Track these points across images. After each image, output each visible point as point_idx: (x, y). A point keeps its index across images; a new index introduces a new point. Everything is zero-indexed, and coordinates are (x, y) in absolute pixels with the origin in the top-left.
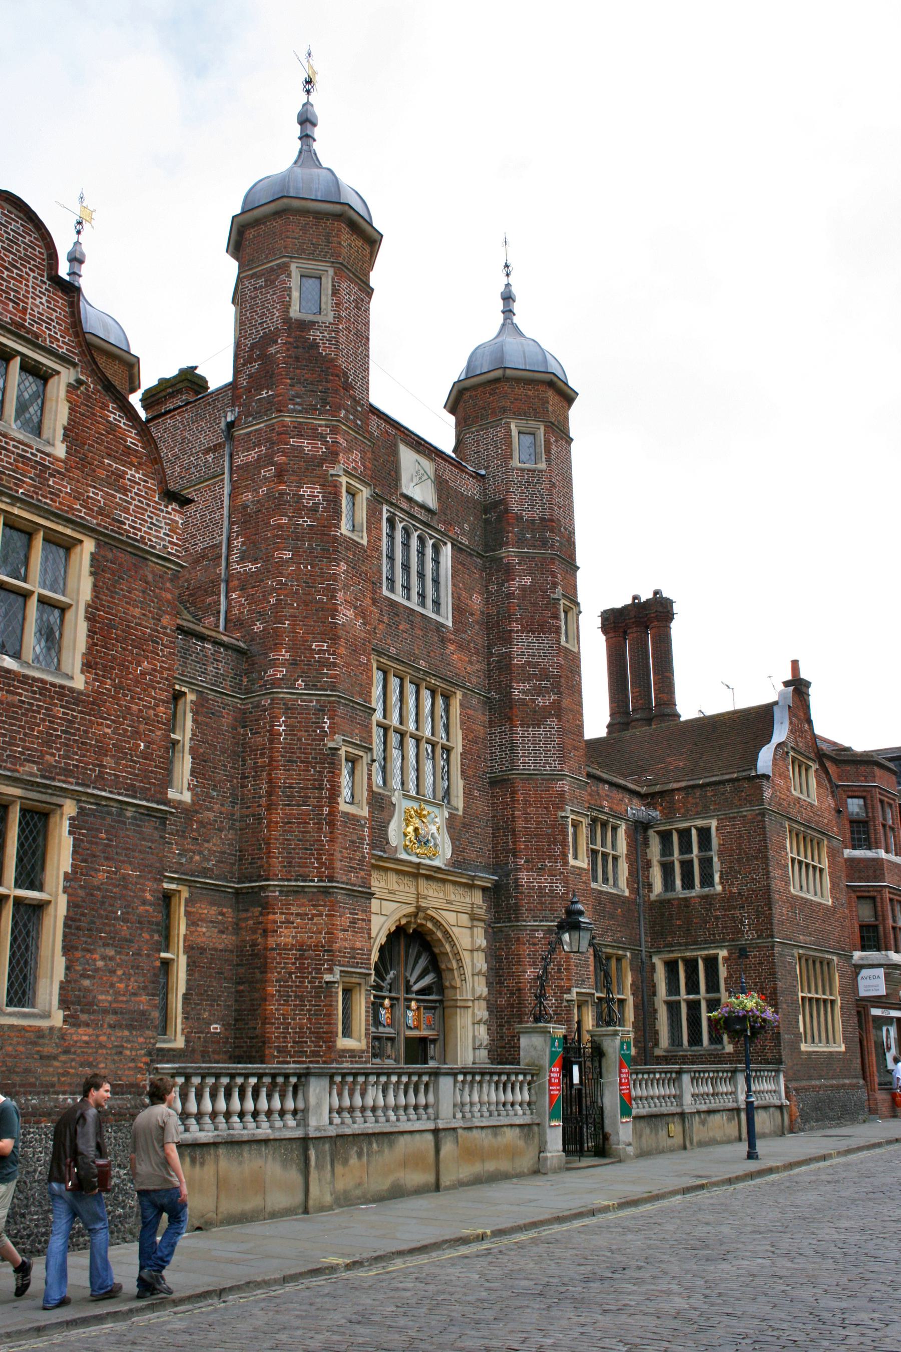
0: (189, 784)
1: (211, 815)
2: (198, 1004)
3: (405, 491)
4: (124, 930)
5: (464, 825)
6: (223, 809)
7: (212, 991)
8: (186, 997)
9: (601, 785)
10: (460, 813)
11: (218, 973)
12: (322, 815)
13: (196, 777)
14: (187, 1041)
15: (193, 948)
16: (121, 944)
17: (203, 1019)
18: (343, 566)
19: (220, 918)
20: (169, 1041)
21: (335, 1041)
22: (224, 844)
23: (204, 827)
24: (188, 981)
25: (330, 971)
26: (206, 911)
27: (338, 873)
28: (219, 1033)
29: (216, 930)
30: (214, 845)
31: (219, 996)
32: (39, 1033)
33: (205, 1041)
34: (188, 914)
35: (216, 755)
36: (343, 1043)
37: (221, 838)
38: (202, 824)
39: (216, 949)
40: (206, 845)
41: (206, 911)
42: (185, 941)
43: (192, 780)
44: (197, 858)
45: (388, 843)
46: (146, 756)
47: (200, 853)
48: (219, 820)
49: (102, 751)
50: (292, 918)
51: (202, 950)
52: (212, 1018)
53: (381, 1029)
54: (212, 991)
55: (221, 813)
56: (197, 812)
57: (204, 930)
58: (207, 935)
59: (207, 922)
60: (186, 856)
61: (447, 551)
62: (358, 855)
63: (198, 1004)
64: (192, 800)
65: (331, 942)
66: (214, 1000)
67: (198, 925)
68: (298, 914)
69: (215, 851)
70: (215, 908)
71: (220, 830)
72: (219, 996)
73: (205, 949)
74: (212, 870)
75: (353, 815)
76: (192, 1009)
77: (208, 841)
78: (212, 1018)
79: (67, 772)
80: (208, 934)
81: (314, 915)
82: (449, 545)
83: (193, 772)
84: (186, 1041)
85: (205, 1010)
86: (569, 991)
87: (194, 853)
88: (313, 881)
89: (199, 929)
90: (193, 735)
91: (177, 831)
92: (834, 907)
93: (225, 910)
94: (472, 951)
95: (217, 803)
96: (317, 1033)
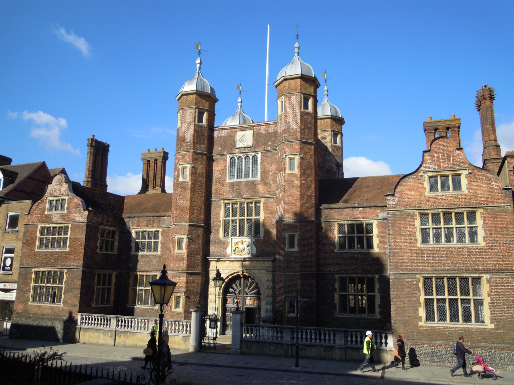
1: (166, 256)
3: (238, 146)
4: (73, 290)
9: (355, 210)
10: (262, 238)
16: (73, 292)
18: (180, 190)
32: (59, 307)
38: (163, 259)
46: (79, 259)
49: (71, 260)
61: (259, 155)
62: (182, 263)
79: (65, 265)
82: (260, 153)
92: (490, 248)
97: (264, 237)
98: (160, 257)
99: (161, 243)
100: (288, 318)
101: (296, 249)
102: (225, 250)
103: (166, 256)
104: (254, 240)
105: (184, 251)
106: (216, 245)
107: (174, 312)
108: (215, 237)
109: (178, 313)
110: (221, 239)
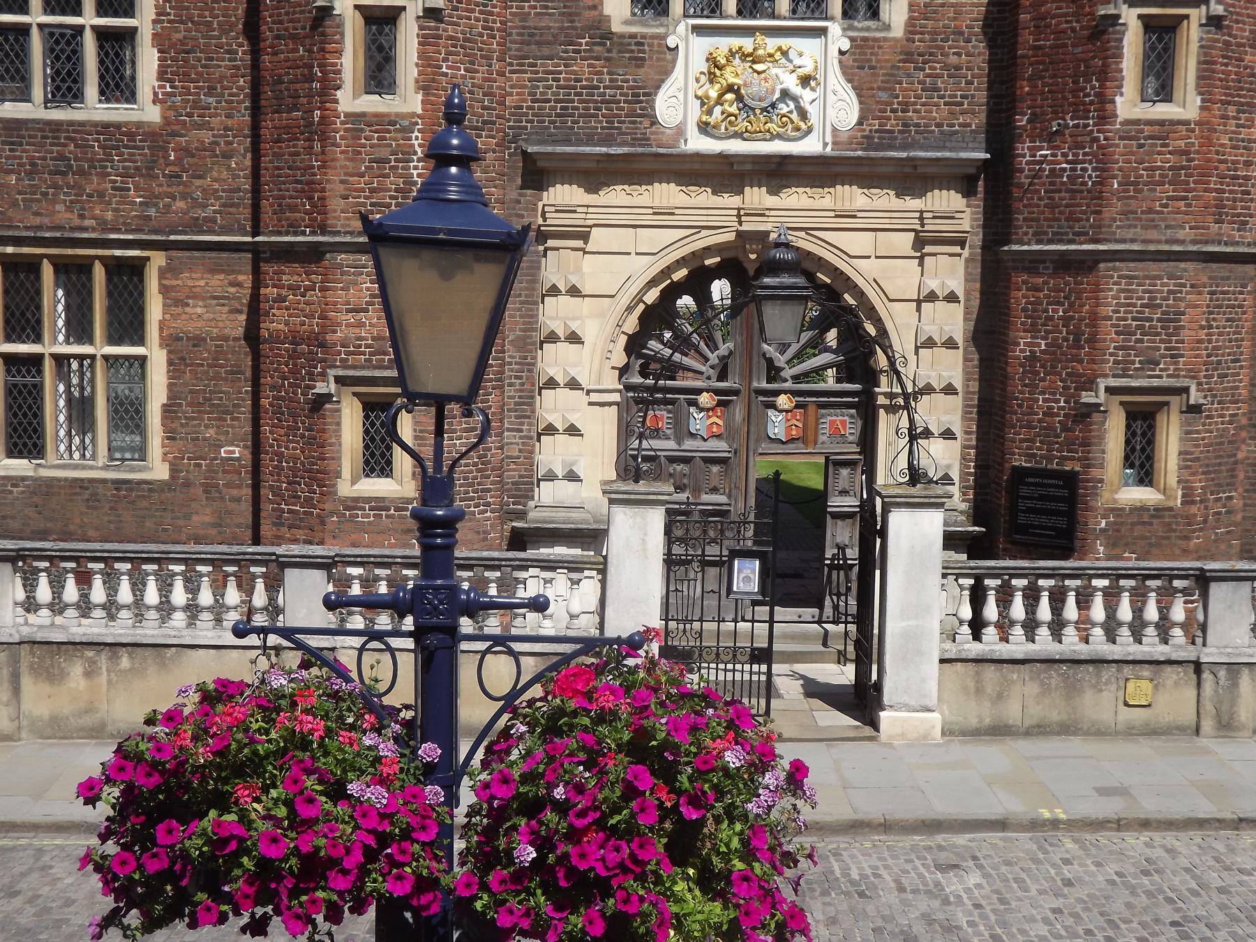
0: (155, 94)
2: (194, 419)
5: (908, 56)
6: (230, 122)
7: (221, 399)
8: (168, 411)
10: (898, 31)
11: (232, 373)
12: (312, 123)
13: (169, 81)
14: (174, 471)
15: (178, 339)
17: (205, 439)
19: (232, 290)
20: (145, 469)
21: (334, 485)
22: (235, 177)
23: (193, 156)
24: (170, 387)
25: (323, 375)
26: (202, 283)
27: (338, 218)
28: (238, 459)
29: (226, 309)
30: (215, 180)
31: (238, 406)
33: (209, 471)
34: (164, 290)
35: (211, 38)
36: (354, 485)
37: (229, 168)
38: (186, 151)
39: (226, 339)
40: (198, 182)
41: (202, 283)
42: (161, 329)
43: (160, 87)
44: (180, 204)
45: (654, 122)
47: (184, 197)
48: (222, 141)
50: (284, 292)
51: (198, 341)
52: (222, 438)
53: (689, 444)
54: (221, 399)
55: (226, 129)
56: (174, 134)
57: (199, 310)
58: (199, 318)
59: (203, 299)
60: (156, 205)
63: (194, 419)
64: (164, 117)
65: (324, 330)
66: (226, 412)
67: (187, 305)
68: (290, 288)
69: (216, 191)
70: (222, 276)
71: (227, 156)
72: (238, 406)
73: (204, 340)
74: (214, 221)
75: (376, 115)
76: (182, 425)
77: (201, 177)
78: (222, 438)
80: (206, 317)
81: (308, 289)
83: (161, 75)
84: (171, 470)
85: (207, 427)
86: (1090, 385)
87: (174, 198)
88: (303, 233)
89: (188, 309)
90: (158, 14)
91: (137, 168)
93: (241, 278)
94: (919, 302)
95: (216, 115)
96: (310, 471)
97: (911, 25)
98: (155, 138)
99: (159, 40)
100: (1118, 511)
101: (1186, 106)
102: (643, 98)
103: (207, 137)
104: (846, 45)
105: (407, 100)
106: (583, 68)
107: (355, 503)
108: (571, 16)
109: (379, 504)
110: (616, 27)
